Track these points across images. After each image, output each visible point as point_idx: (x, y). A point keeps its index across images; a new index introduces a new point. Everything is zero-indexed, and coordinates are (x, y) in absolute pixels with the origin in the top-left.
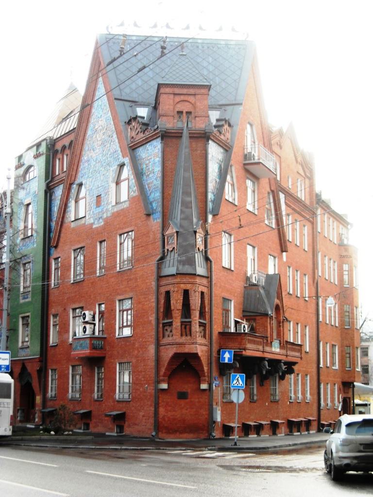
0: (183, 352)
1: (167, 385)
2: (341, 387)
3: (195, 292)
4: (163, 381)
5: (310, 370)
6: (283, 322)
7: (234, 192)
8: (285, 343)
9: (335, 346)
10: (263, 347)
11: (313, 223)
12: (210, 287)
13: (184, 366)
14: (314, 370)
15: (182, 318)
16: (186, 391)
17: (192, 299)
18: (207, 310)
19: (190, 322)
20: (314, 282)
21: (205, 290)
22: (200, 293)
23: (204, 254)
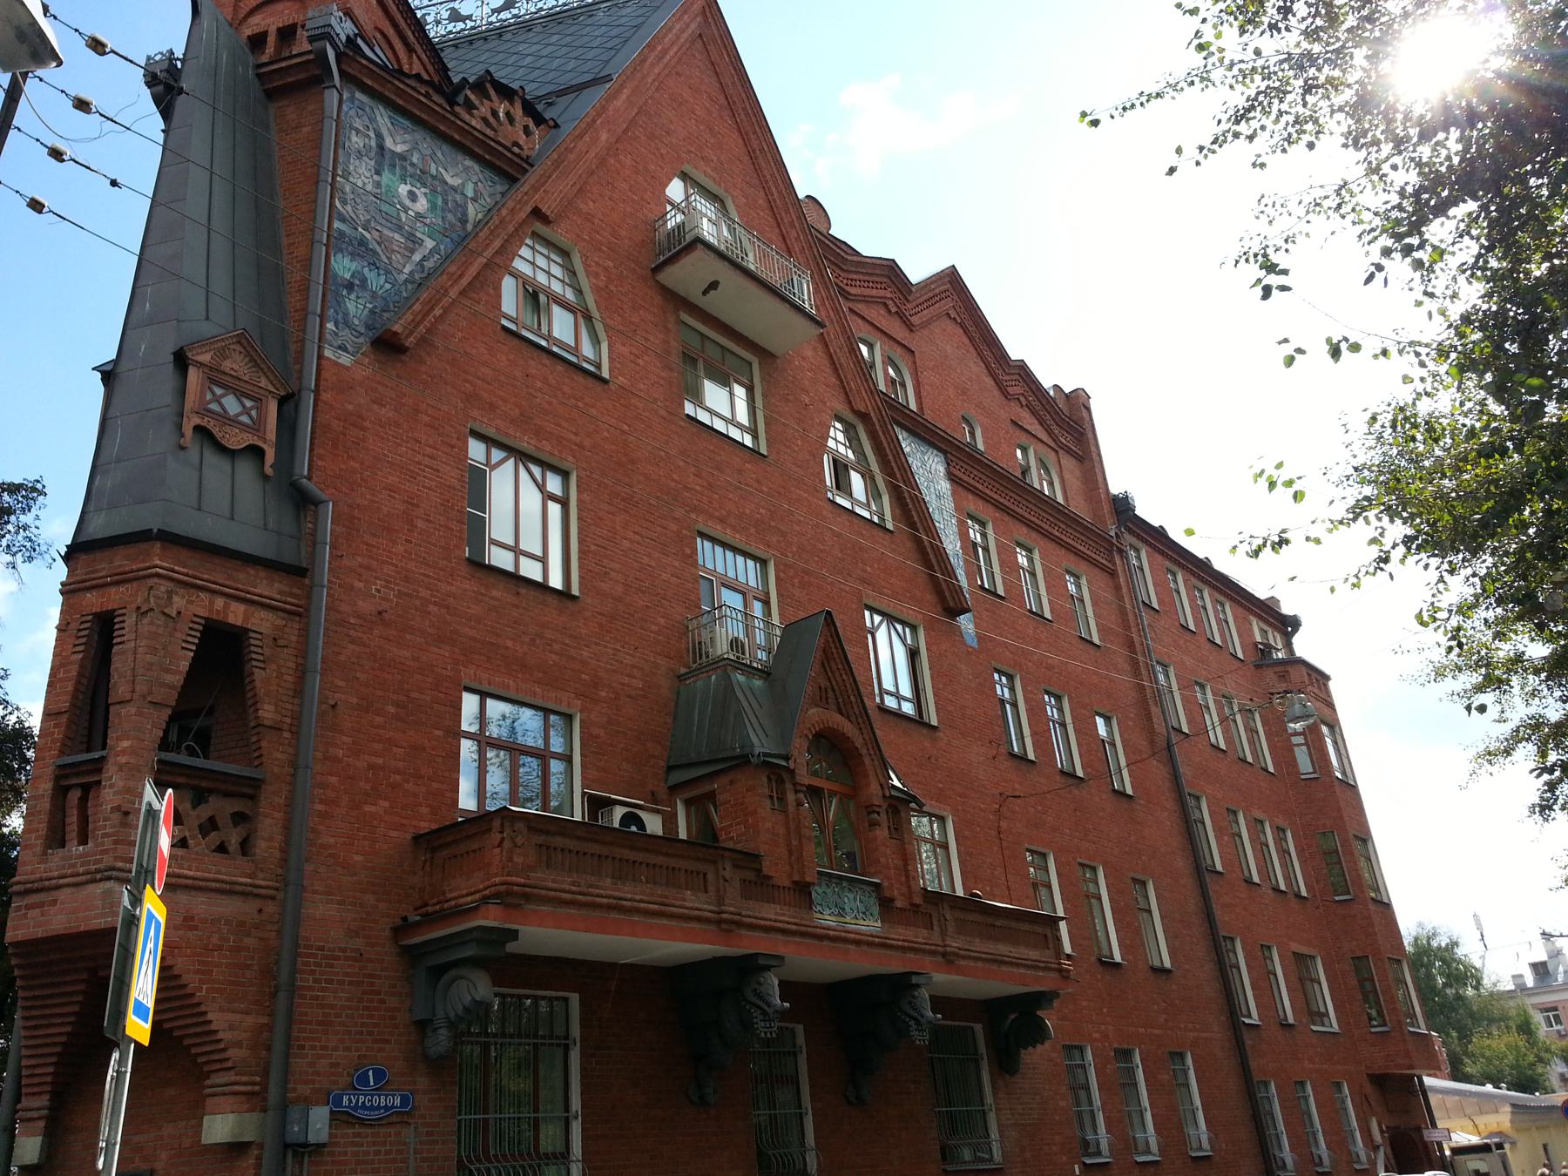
0: (40, 933)
2: (1369, 1089)
5: (1191, 1035)
7: (599, 343)
8: (918, 900)
9: (1313, 958)
10: (720, 900)
11: (1112, 574)
12: (300, 614)
14: (1217, 1032)
15: (62, 753)
16: (144, 1167)
17: (123, 653)
18: (267, 712)
19: (98, 766)
20: (1152, 742)
21: (262, 622)
23: (268, 470)
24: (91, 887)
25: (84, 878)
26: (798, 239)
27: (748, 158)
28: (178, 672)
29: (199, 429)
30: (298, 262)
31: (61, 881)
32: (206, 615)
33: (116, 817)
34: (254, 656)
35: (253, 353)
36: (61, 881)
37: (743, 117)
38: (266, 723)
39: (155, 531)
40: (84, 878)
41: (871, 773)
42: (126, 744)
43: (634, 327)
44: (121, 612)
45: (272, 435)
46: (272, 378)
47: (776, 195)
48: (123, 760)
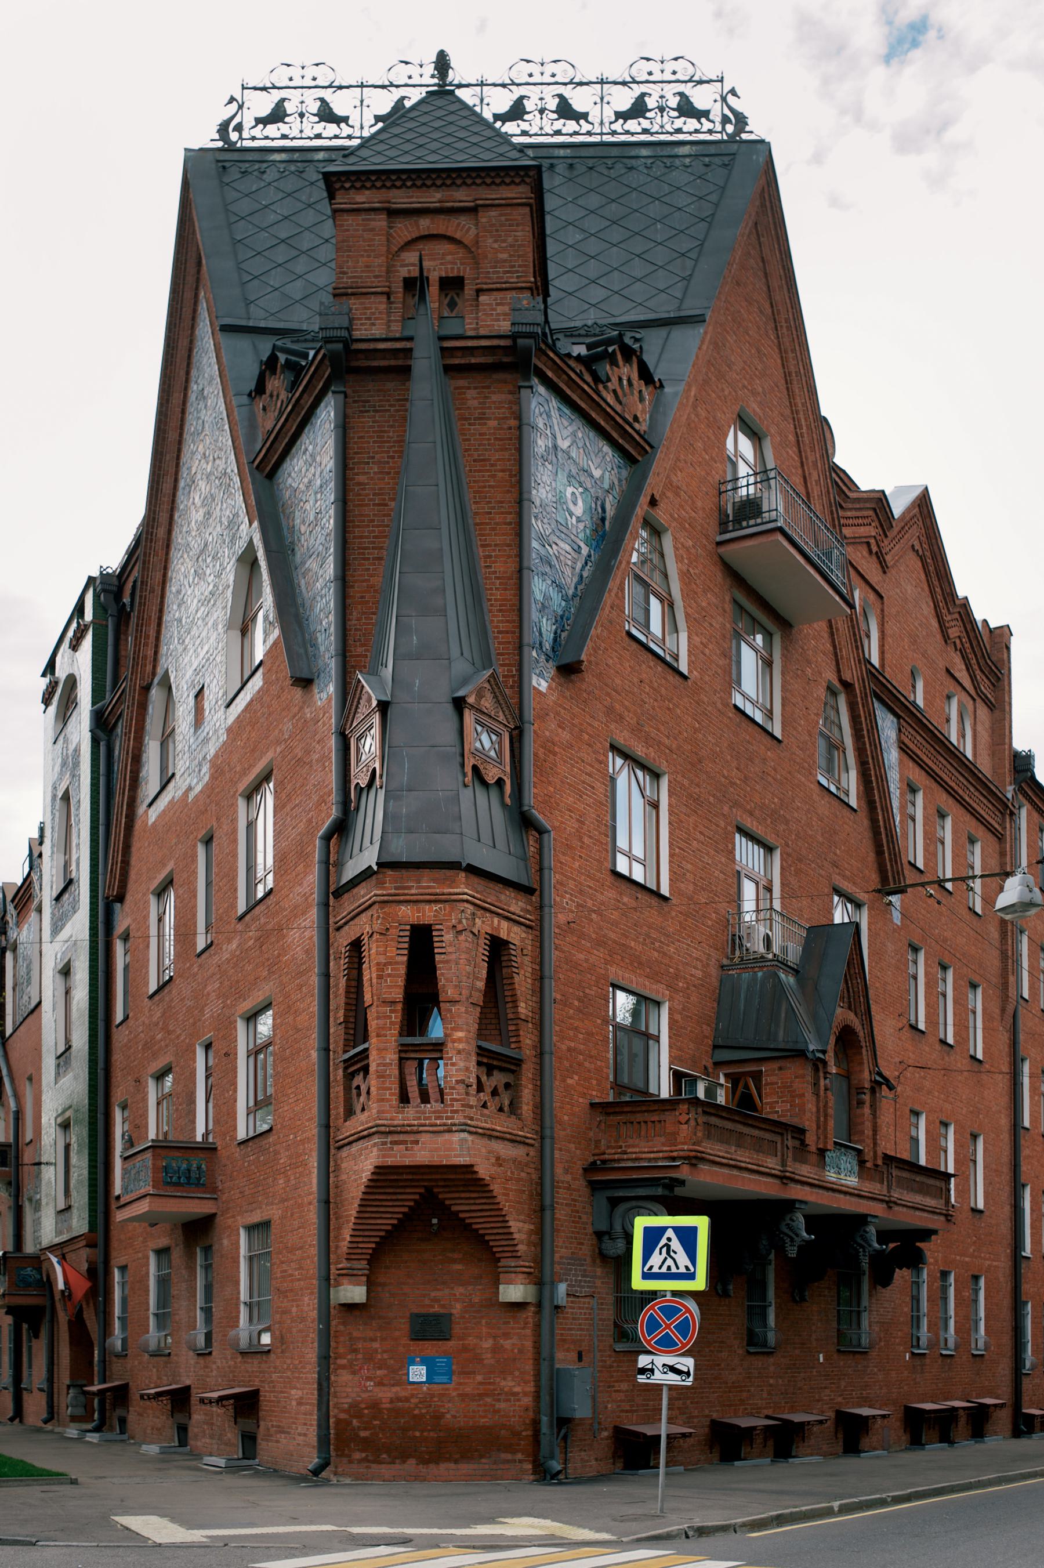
0: (407, 1162)
1: (363, 1290)
3: (460, 932)
4: (350, 1275)
6: (873, 1091)
13: (435, 1221)
17: (447, 962)
22: (482, 941)
23: (508, 801)
24: (447, 1136)
25: (442, 1128)
26: (818, 482)
27: (783, 382)
28: (480, 980)
29: (475, 768)
30: (497, 578)
31: (421, 1129)
32: (490, 932)
33: (461, 1088)
34: (514, 964)
35: (496, 690)
36: (421, 1129)
37: (785, 330)
38: (523, 1017)
39: (464, 865)
40: (442, 1128)
41: (866, 1062)
42: (460, 1034)
43: (704, 614)
44: (438, 927)
45: (508, 769)
46: (507, 713)
47: (804, 430)
48: (461, 1046)
